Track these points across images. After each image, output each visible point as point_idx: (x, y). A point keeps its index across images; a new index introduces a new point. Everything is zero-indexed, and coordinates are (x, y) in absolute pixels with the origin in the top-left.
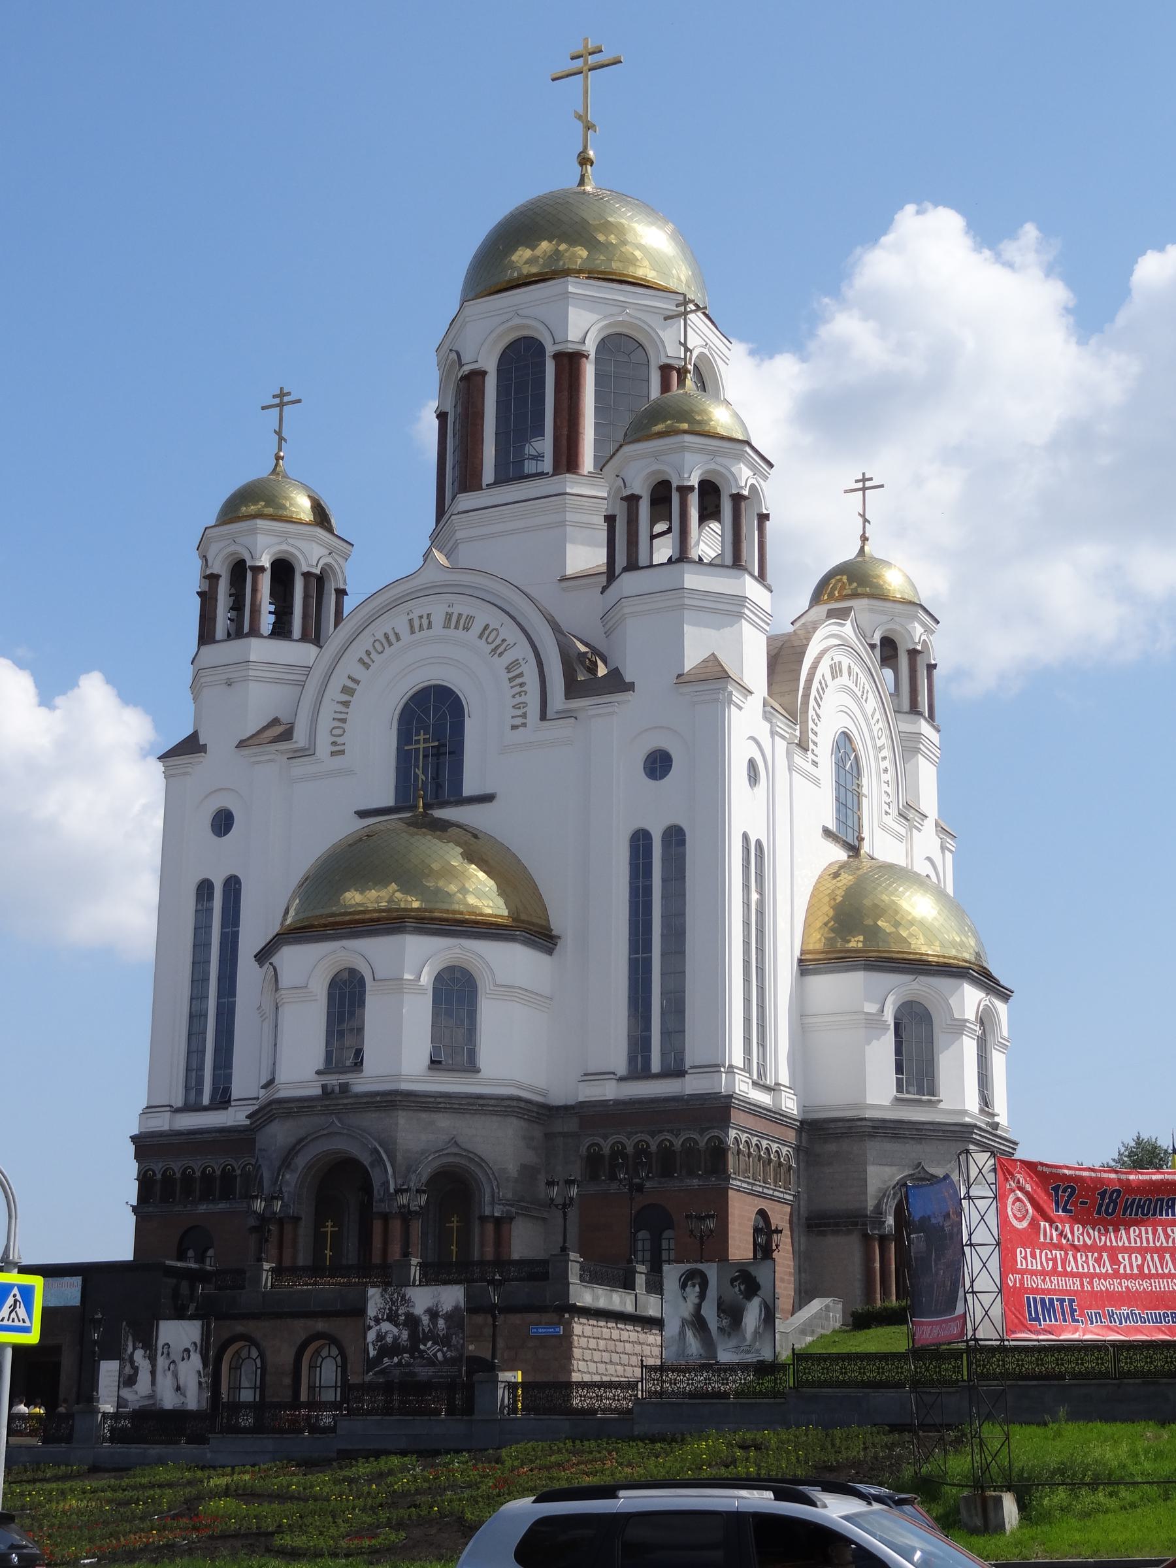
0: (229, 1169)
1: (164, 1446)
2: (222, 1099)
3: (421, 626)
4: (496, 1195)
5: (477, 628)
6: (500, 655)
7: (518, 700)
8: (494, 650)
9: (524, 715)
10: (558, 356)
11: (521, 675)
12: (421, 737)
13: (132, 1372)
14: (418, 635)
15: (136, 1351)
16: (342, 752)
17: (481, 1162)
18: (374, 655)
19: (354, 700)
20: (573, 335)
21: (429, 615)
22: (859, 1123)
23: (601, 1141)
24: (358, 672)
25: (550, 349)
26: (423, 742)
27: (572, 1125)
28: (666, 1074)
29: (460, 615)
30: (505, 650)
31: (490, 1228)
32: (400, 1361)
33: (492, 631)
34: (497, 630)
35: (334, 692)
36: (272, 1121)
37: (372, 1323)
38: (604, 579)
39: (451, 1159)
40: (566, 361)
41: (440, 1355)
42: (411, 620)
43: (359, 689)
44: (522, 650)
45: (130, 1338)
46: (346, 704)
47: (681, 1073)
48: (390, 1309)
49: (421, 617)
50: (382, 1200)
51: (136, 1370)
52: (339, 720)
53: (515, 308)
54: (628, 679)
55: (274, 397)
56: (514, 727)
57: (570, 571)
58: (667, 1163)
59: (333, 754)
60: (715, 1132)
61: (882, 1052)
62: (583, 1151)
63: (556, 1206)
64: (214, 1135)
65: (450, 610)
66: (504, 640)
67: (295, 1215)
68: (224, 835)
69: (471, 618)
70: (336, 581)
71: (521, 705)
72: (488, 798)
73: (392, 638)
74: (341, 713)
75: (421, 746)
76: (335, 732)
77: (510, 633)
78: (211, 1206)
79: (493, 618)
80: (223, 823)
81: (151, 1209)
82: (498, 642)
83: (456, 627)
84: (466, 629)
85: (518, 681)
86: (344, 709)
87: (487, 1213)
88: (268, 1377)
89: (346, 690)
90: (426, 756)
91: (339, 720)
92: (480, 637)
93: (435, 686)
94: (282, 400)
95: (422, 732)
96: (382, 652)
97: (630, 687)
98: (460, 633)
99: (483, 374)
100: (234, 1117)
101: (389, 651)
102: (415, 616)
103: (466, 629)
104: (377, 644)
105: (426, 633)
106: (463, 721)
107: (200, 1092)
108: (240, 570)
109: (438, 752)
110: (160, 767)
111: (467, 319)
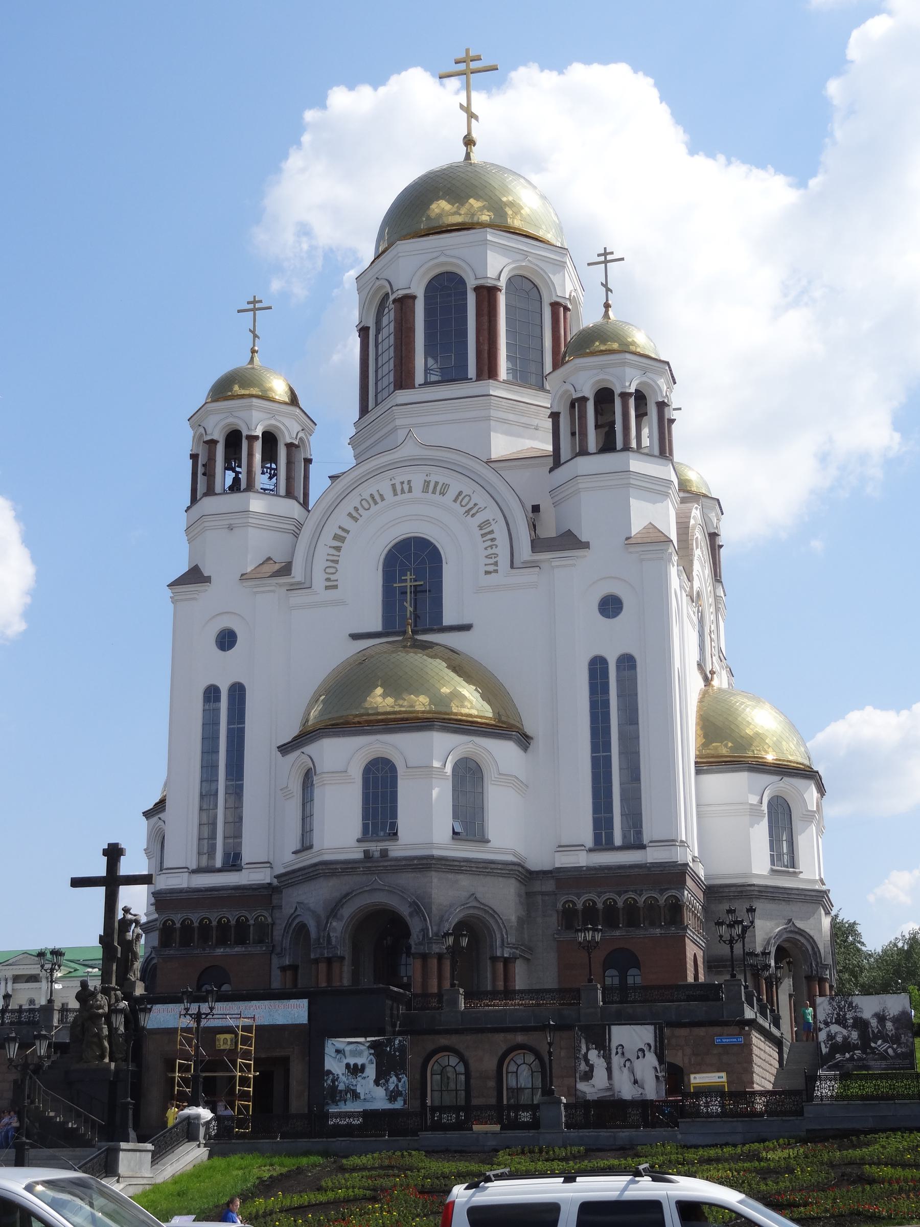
1: (634, 1130)
2: (233, 863)
3: (402, 489)
4: (506, 940)
5: (451, 493)
6: (473, 516)
7: (490, 551)
8: (468, 512)
9: (496, 564)
10: (478, 289)
11: (492, 532)
12: (408, 577)
13: (587, 1069)
14: (400, 497)
15: (590, 1052)
16: (335, 587)
17: (494, 914)
18: (361, 511)
19: (345, 546)
20: (491, 273)
21: (409, 482)
22: (749, 888)
23: (575, 899)
24: (348, 524)
25: (471, 283)
26: (409, 580)
27: (550, 886)
28: (626, 847)
29: (437, 483)
30: (477, 512)
31: (500, 966)
32: (852, 1057)
33: (465, 497)
34: (469, 496)
35: (327, 538)
36: (313, 879)
37: (822, 1026)
38: (551, 460)
39: (471, 911)
40: (485, 293)
41: (890, 1051)
42: (393, 485)
43: (349, 537)
44: (491, 513)
45: (583, 1041)
46: (338, 549)
47: (642, 847)
48: (838, 1014)
49: (402, 483)
50: (420, 944)
51: (592, 1067)
52: (332, 561)
53: (442, 249)
54: (584, 539)
55: (249, 303)
56: (487, 573)
57: (494, 456)
58: (633, 917)
59: (327, 588)
60: (673, 892)
61: (760, 833)
62: (560, 906)
63: (724, 942)
64: (230, 892)
65: (428, 479)
66: (475, 505)
67: (342, 955)
68: (228, 650)
69: (446, 486)
70: (305, 451)
71: (493, 556)
72: (467, 628)
73: (377, 497)
74: (333, 555)
75: (409, 584)
76: (328, 570)
77: (480, 498)
78: (228, 950)
79: (466, 487)
80: (226, 640)
81: (172, 952)
82: (471, 505)
83: (434, 492)
84: (442, 494)
85: (489, 537)
86: (337, 553)
87: (499, 954)
88: (472, 1081)
89: (336, 537)
90: (411, 592)
91: (332, 561)
92: (455, 501)
93: (415, 538)
94: (255, 306)
95: (409, 573)
96: (368, 509)
97: (586, 545)
98: (437, 497)
99: (413, 298)
100: (261, 877)
101: (374, 508)
102: (397, 481)
103: (442, 494)
104: (364, 503)
105: (407, 496)
106: (442, 566)
108: (234, 439)
109: (417, 591)
110: (168, 593)
111: (400, 255)
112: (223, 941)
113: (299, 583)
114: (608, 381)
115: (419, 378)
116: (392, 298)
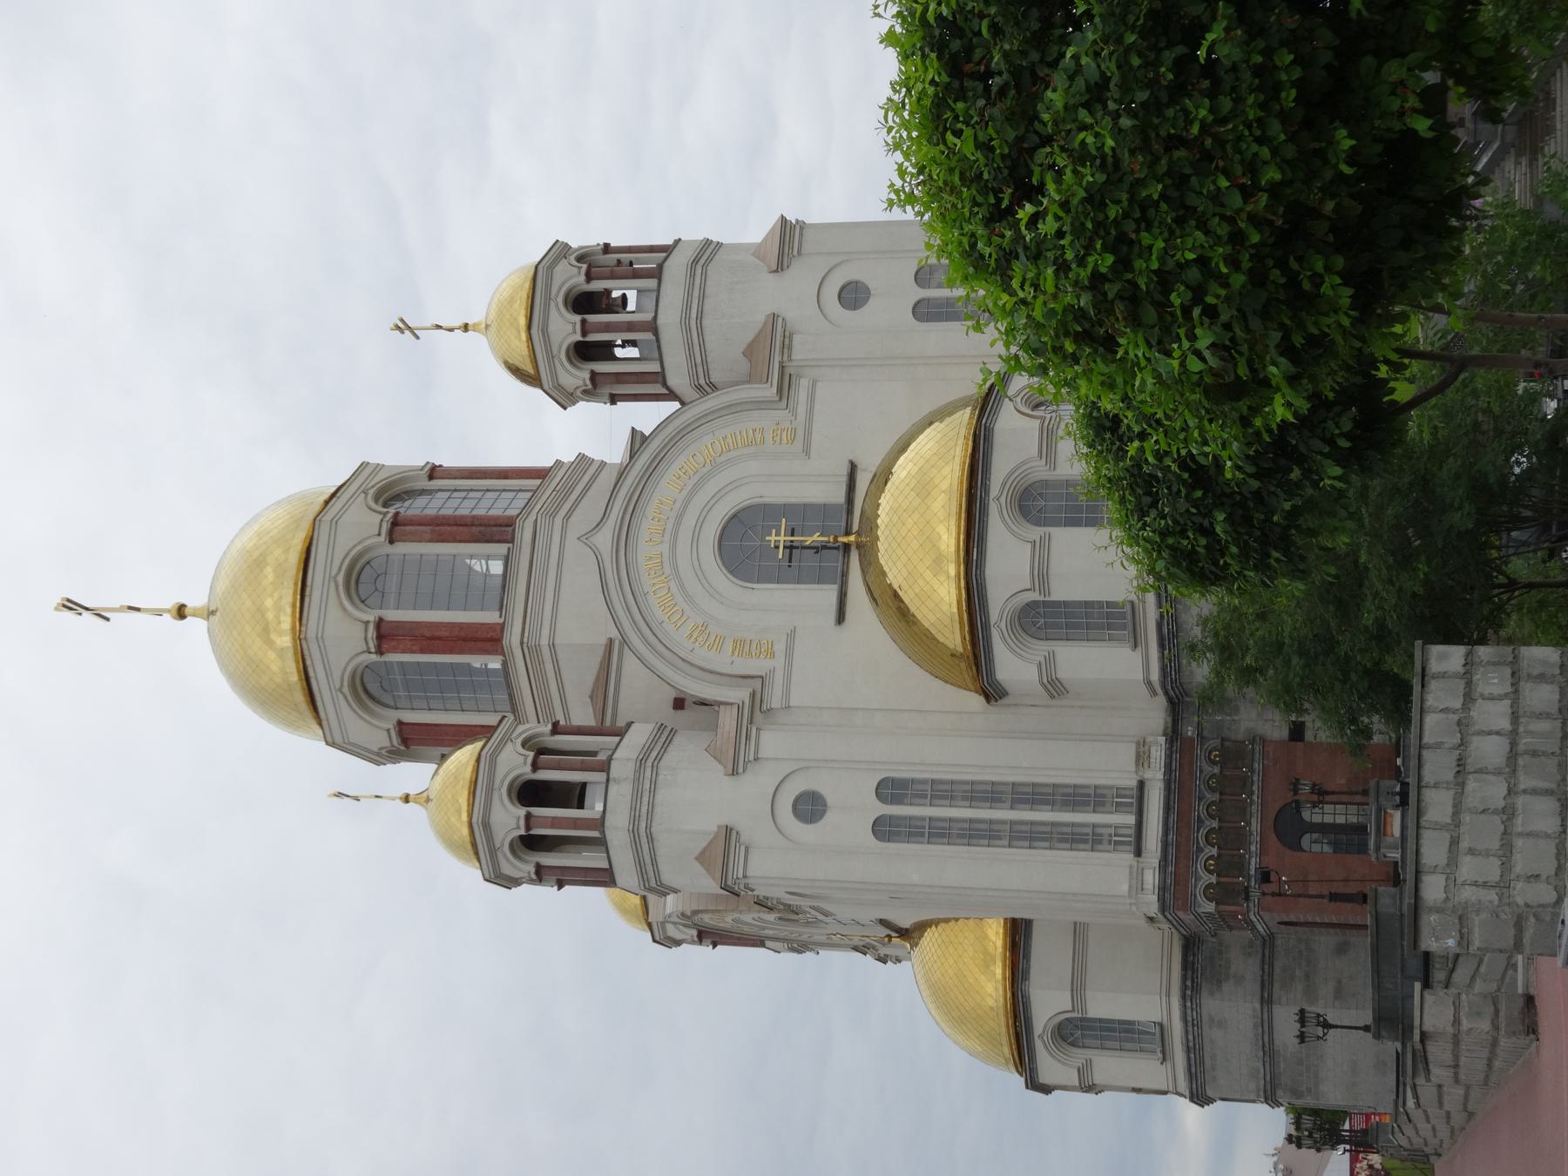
72: (853, 468)
90: (792, 541)
113: (753, 695)
115: (491, 617)
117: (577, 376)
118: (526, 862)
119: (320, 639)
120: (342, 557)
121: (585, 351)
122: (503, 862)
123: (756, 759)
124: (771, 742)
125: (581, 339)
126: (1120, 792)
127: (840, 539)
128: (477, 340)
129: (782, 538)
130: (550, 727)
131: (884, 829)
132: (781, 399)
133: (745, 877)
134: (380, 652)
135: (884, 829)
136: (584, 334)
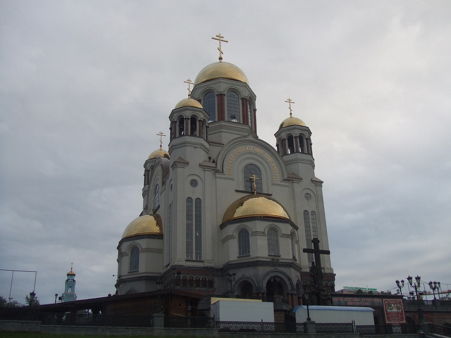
0: (204, 279)
107: (191, 256)
112: (198, 286)
113: (219, 170)
114: (292, 134)
115: (226, 119)
116: (216, 94)
117: (284, 135)
118: (177, 119)
119: (220, 82)
120: (237, 87)
121: (290, 138)
122: (177, 114)
123: (205, 170)
124: (209, 174)
125: (293, 137)
126: (200, 257)
127: (255, 192)
128: (289, 116)
129: (254, 178)
130: (207, 126)
131: (189, 200)
132: (284, 179)
133: (177, 167)
134: (217, 95)
135: (189, 200)
136: (295, 137)
